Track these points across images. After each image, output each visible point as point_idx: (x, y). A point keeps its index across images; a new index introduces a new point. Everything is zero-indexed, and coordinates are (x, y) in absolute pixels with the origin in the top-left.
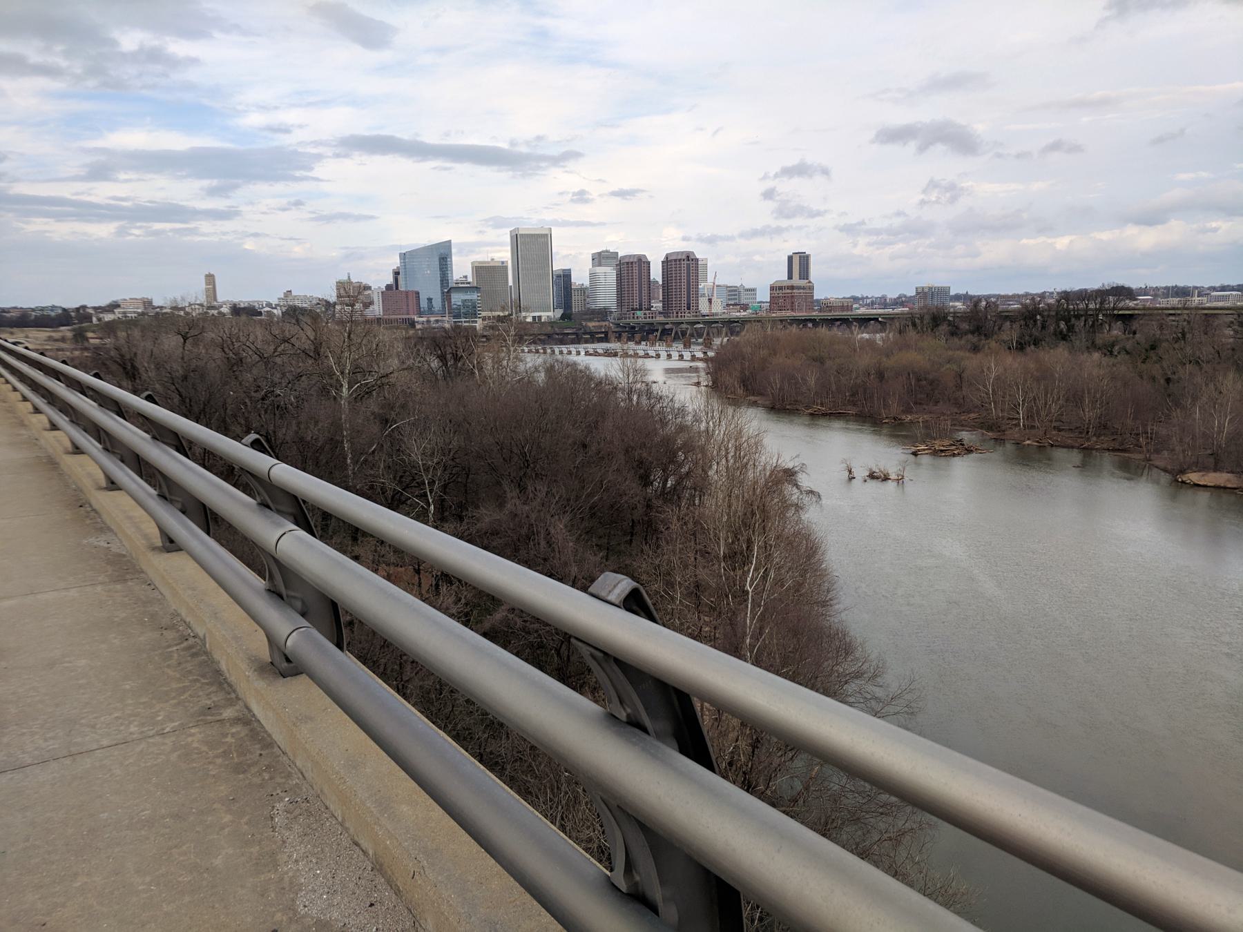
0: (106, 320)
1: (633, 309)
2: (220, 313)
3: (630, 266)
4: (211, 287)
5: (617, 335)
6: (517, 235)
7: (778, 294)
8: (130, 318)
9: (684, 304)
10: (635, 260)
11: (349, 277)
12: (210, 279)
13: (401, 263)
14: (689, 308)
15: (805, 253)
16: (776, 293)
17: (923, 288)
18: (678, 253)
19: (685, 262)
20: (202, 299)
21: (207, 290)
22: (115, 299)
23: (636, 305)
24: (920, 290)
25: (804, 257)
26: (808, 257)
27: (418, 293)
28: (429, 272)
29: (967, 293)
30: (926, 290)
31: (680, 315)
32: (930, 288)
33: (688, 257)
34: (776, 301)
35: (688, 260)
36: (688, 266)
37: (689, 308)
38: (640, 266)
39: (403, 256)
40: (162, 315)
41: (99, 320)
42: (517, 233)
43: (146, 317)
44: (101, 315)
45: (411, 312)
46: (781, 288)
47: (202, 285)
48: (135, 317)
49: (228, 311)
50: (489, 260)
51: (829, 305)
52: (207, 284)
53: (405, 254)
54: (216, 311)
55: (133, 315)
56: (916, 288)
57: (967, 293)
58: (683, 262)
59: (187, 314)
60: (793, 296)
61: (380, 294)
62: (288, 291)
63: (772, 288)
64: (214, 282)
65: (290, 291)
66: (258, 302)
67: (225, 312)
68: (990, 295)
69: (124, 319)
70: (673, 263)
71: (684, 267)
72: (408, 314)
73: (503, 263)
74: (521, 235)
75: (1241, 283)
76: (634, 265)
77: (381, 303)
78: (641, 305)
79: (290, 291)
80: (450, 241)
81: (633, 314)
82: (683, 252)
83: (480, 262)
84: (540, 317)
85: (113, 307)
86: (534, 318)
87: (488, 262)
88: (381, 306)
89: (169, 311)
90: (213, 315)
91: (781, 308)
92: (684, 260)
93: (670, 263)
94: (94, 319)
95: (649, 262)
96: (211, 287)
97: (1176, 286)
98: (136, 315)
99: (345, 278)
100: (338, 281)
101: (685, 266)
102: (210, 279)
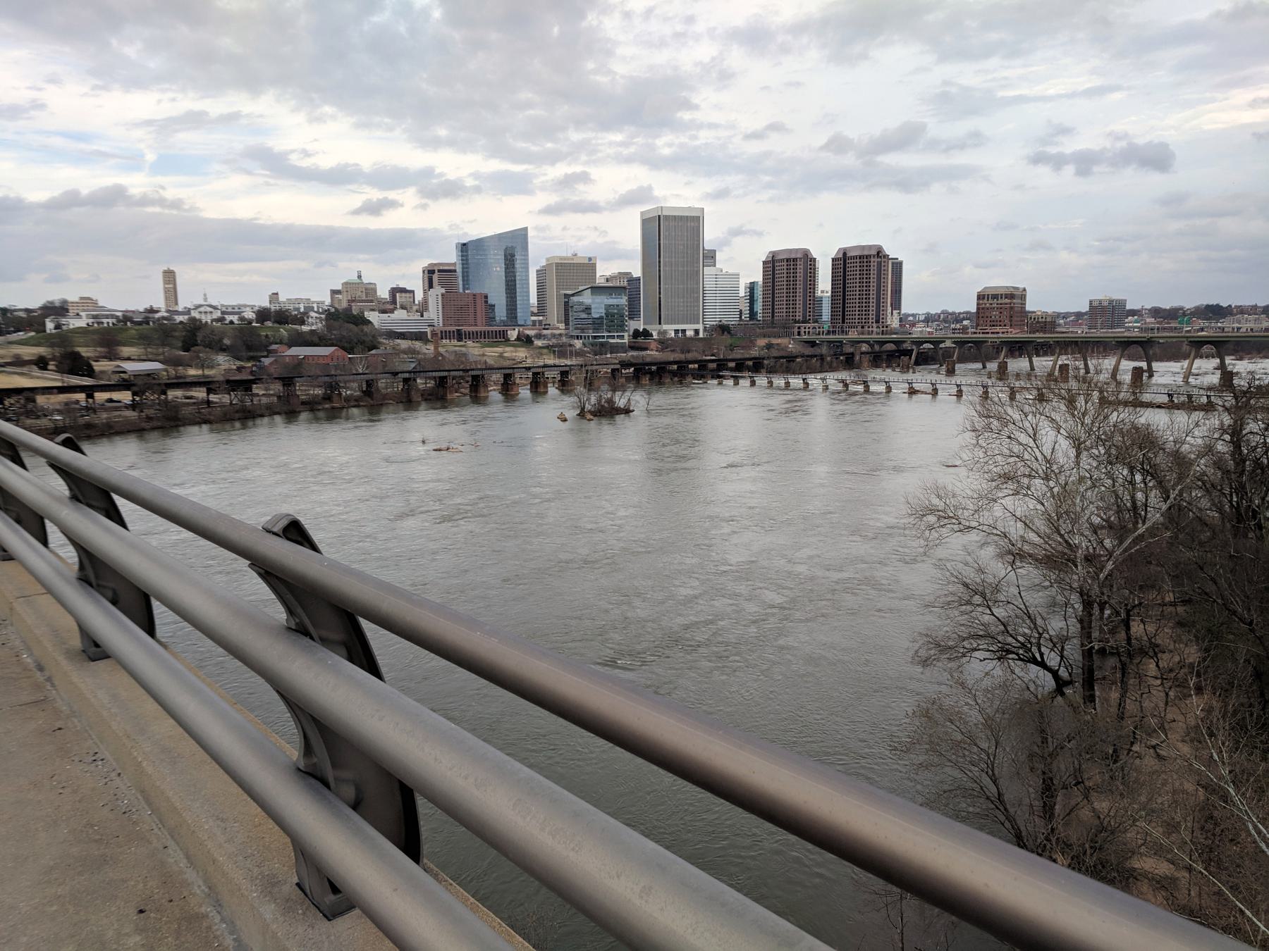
0: (71, 327)
1: (796, 322)
2: (242, 319)
3: (792, 263)
4: (171, 286)
5: (871, 359)
6: (659, 216)
8: (105, 325)
9: (872, 316)
10: (799, 256)
11: (359, 277)
12: (170, 276)
13: (458, 256)
14: (877, 322)
15: (897, 259)
17: (1100, 301)
18: (863, 247)
19: (876, 260)
20: (158, 301)
21: (166, 291)
22: (50, 299)
23: (799, 316)
24: (1095, 304)
25: (897, 263)
26: (901, 263)
27: (486, 297)
28: (498, 269)
30: (1106, 304)
31: (866, 328)
32: (1111, 301)
33: (878, 253)
36: (879, 264)
37: (877, 322)
39: (464, 247)
40: (154, 322)
41: (58, 327)
42: (660, 214)
43: (129, 324)
44: (63, 321)
45: (479, 322)
46: (995, 297)
47: (159, 285)
48: (113, 324)
49: (254, 316)
50: (569, 255)
51: (1040, 320)
52: (166, 282)
53: (464, 244)
54: (236, 317)
55: (110, 321)
56: (1091, 302)
58: (872, 260)
59: (193, 320)
60: (1011, 308)
61: (440, 297)
62: (273, 294)
63: (981, 297)
64: (175, 280)
65: (277, 294)
66: (299, 301)
67: (250, 317)
69: (96, 325)
70: (858, 260)
72: (476, 325)
73: (590, 259)
74: (665, 216)
77: (440, 306)
78: (804, 316)
79: (277, 294)
80: (526, 229)
81: (799, 328)
82: (870, 247)
83: (561, 258)
84: (683, 331)
85: (58, 310)
86: (677, 331)
87: (573, 259)
88: (440, 312)
89: (166, 314)
90: (232, 322)
91: (999, 323)
92: (874, 256)
93: (843, 263)
94: (50, 326)
96: (171, 286)
98: (114, 321)
99: (354, 278)
100: (345, 281)
102: (170, 276)
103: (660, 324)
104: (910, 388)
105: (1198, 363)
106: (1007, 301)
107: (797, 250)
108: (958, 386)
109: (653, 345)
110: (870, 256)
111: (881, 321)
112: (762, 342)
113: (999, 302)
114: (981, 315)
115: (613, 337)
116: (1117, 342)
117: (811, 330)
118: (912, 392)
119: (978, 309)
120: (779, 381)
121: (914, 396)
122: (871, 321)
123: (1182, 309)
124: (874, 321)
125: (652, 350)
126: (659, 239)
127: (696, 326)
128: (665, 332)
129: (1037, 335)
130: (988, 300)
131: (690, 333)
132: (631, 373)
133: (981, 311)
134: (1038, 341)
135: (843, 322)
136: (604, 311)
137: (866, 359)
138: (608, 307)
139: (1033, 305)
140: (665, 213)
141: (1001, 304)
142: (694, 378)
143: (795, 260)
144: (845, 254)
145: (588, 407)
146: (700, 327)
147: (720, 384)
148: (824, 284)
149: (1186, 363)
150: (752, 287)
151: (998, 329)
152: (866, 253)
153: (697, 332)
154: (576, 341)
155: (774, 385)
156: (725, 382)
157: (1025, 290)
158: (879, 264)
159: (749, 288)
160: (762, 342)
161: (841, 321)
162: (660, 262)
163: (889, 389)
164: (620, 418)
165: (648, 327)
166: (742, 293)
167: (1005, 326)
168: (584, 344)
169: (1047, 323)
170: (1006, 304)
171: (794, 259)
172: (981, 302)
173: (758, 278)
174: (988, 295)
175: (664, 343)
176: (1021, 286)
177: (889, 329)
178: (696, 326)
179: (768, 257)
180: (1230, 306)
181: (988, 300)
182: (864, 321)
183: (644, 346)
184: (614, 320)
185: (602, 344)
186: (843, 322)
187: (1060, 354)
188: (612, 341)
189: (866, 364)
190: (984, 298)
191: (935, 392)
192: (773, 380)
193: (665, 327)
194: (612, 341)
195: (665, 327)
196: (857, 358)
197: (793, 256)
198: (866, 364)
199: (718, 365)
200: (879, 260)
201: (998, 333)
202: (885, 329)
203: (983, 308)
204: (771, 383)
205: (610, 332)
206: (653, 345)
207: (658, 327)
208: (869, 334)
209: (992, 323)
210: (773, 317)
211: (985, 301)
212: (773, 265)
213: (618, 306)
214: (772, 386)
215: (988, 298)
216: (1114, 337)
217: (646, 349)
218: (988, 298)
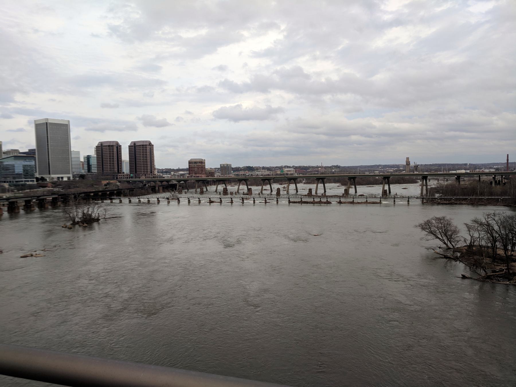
7: (194, 166)
9: (149, 171)
10: (114, 144)
14: (151, 173)
16: (193, 165)
17: (224, 164)
18: (143, 141)
19: (149, 147)
24: (222, 166)
29: (179, 168)
30: (226, 166)
32: (227, 165)
34: (193, 169)
35: (150, 146)
36: (150, 148)
37: (151, 173)
38: (117, 147)
46: (195, 163)
56: (221, 165)
57: (179, 168)
58: (147, 147)
60: (202, 167)
63: (190, 162)
68: (170, 169)
71: (148, 149)
75: (515, 162)
76: (114, 147)
84: (62, 178)
86: (58, 178)
92: (148, 145)
93: (134, 148)
95: (121, 146)
97: (259, 167)
101: (149, 148)
103: (50, 174)
104: (210, 200)
105: (264, 187)
106: (200, 164)
107: (113, 142)
108: (199, 198)
109: (50, 185)
110: (146, 145)
111: (153, 172)
112: (104, 182)
113: (197, 165)
114: (190, 170)
115: (28, 181)
116: (238, 180)
117: (122, 176)
118: (211, 202)
119: (189, 167)
120: (135, 200)
121: (212, 204)
122: (148, 172)
123: (239, 168)
124: (150, 172)
125: (49, 187)
126: (47, 134)
127: (69, 175)
128: (53, 178)
129: (210, 177)
130: (193, 164)
131: (65, 179)
132: (50, 200)
133: (190, 168)
134: (208, 180)
135: (136, 173)
136: (22, 168)
137: (161, 188)
138: (24, 166)
139: (209, 165)
140: (49, 122)
141: (198, 165)
142: (95, 201)
143: (112, 146)
144: (135, 144)
145: (77, 220)
146: (71, 175)
147: (112, 202)
148: (125, 156)
149: (260, 187)
150: (88, 158)
151: (198, 175)
152: (145, 144)
153: (69, 178)
154: (5, 184)
155: (141, 202)
156: (114, 201)
157: (205, 160)
158: (150, 148)
159: (87, 158)
160: (104, 182)
161: (134, 173)
162: (48, 145)
163: (200, 201)
164: (95, 224)
165: (44, 176)
166: (82, 160)
167: (200, 174)
168: (9, 185)
169: (211, 173)
170: (200, 165)
171: (112, 146)
172: (190, 164)
173: (92, 153)
174: (193, 162)
175: (55, 184)
176: (203, 159)
177: (156, 176)
178: (69, 175)
179: (98, 144)
180: (290, 166)
181: (193, 164)
182: (145, 172)
183: (44, 185)
184: (28, 173)
185: (22, 185)
186: (136, 173)
187: (218, 184)
188: (28, 183)
189: (161, 191)
190: (191, 163)
191: (221, 202)
192: (131, 199)
193: (52, 176)
194: (28, 183)
195: (52, 176)
196: (157, 188)
197: (112, 144)
198: (161, 191)
199: (102, 193)
200: (150, 147)
201: (199, 177)
202: (154, 176)
203: (191, 167)
204: (130, 201)
205: (26, 178)
206: (50, 185)
207: (48, 176)
208: (148, 178)
209: (195, 173)
210: (103, 172)
211: (192, 164)
212: (101, 148)
213: (30, 165)
214: (140, 202)
215: (193, 163)
216: (237, 178)
217: (46, 187)
218: (193, 163)
